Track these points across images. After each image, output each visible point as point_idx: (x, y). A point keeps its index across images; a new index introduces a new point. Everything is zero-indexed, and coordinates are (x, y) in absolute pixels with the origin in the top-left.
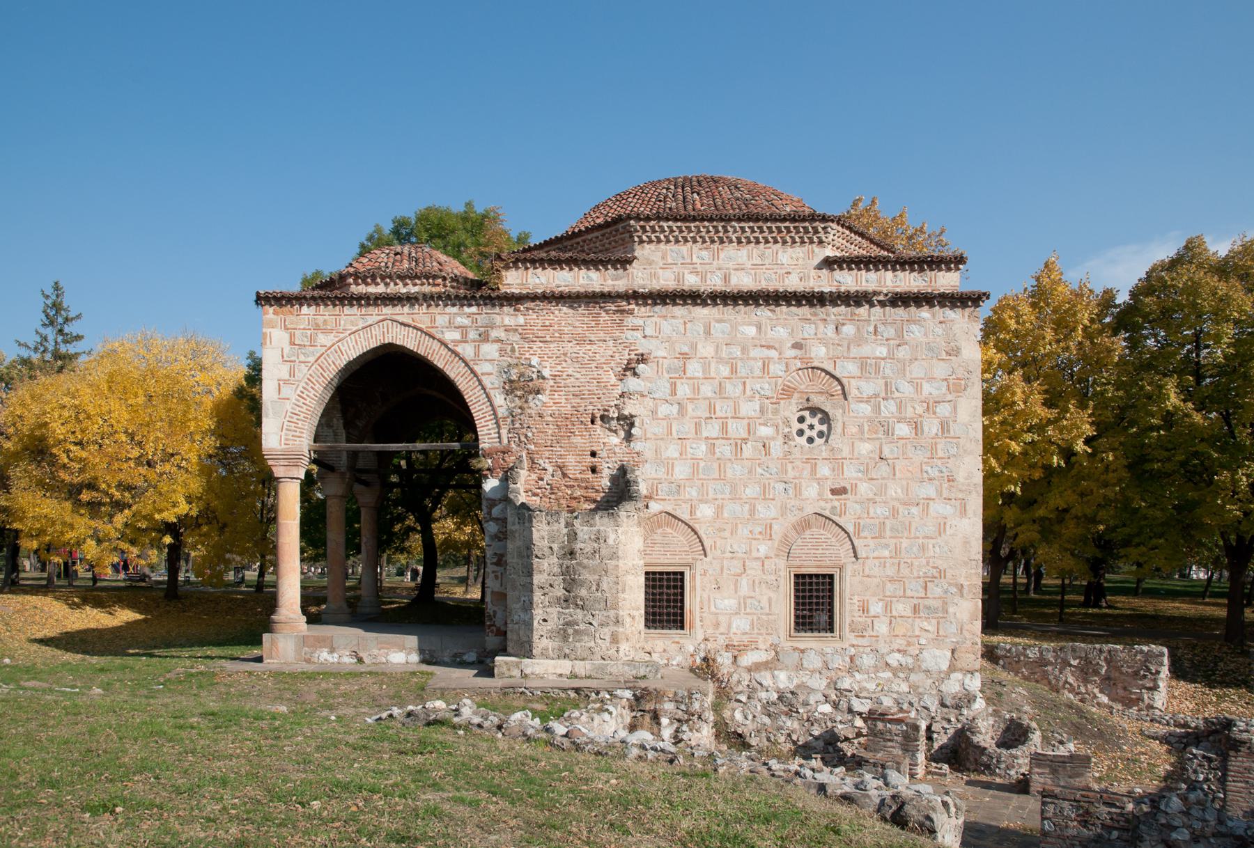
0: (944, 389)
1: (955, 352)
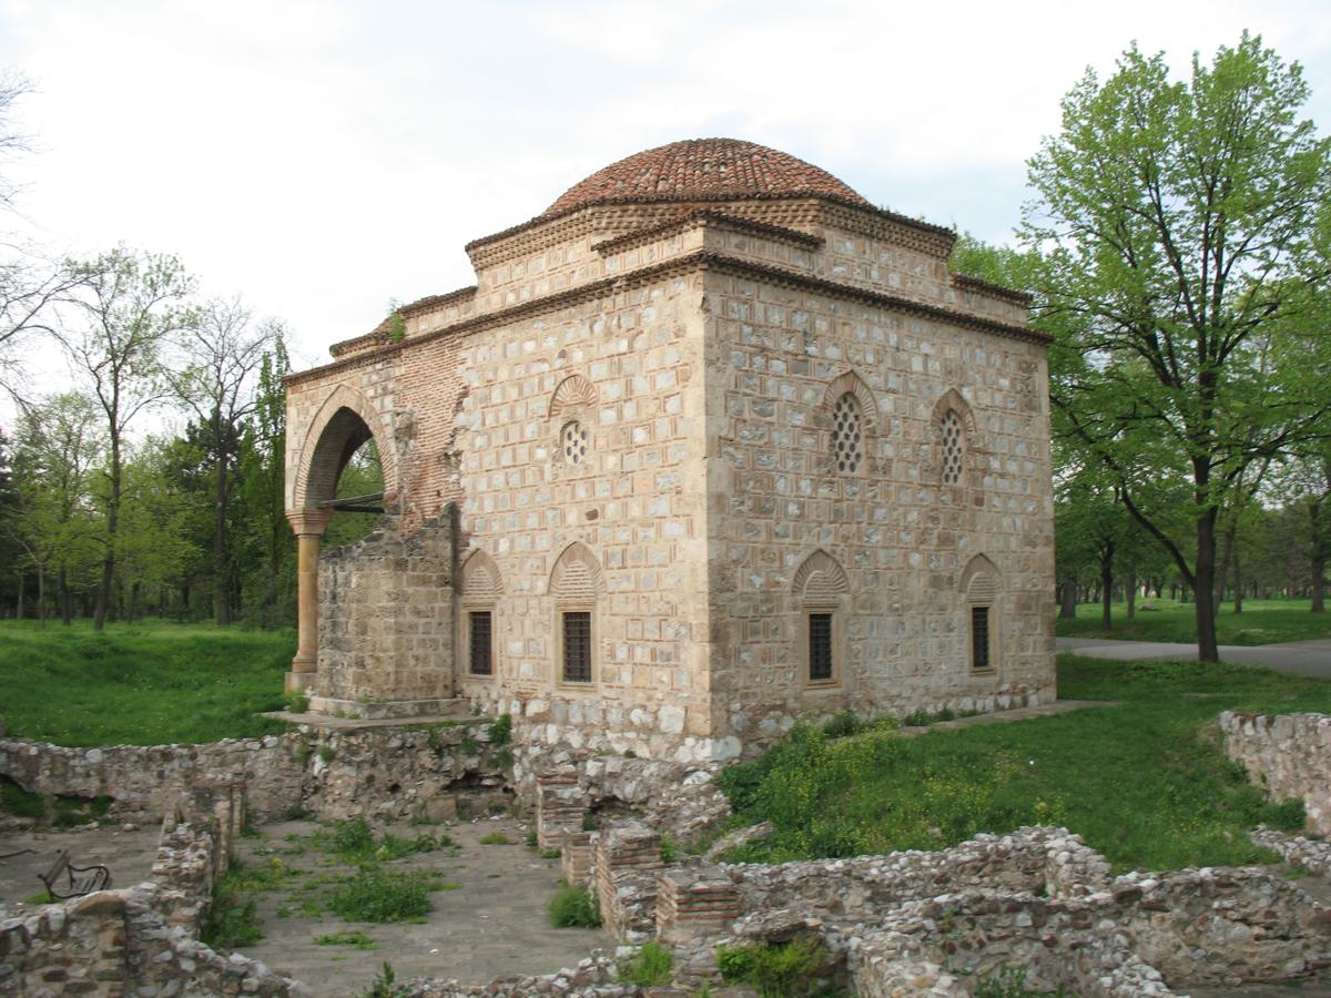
0: (673, 381)
1: (680, 332)
